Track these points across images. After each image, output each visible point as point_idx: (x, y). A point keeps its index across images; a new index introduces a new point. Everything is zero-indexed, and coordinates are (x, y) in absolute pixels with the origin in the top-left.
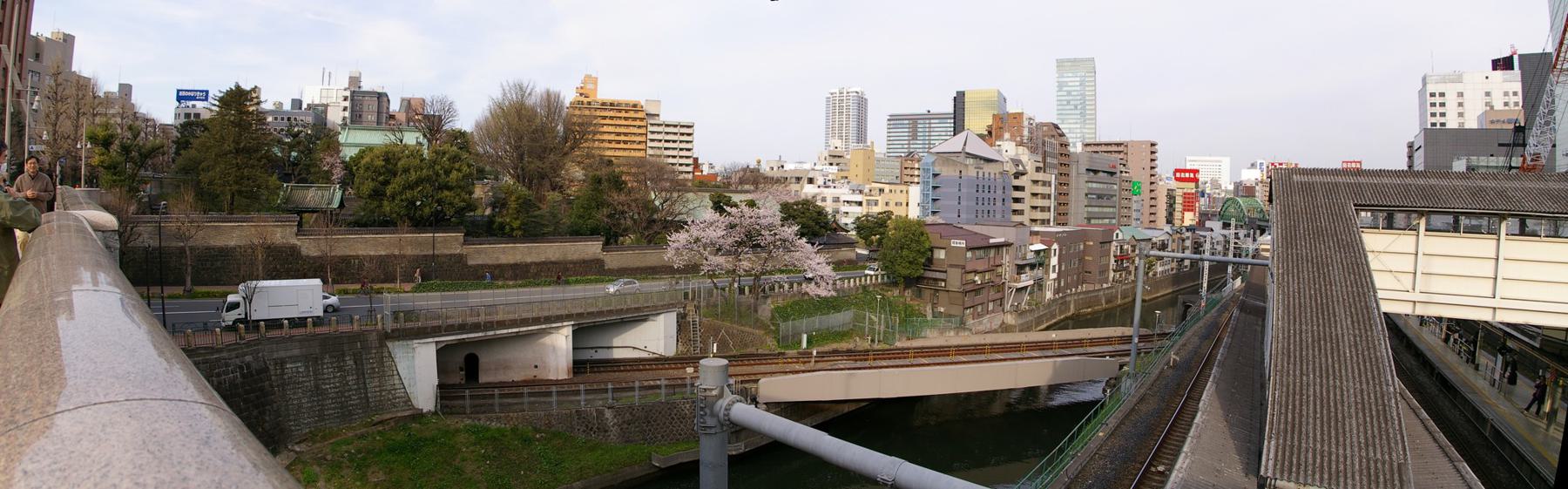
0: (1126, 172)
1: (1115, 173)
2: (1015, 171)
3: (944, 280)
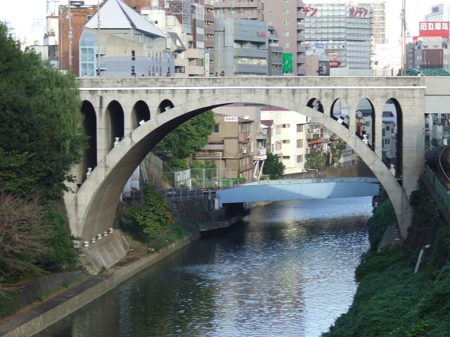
0: (275, 41)
1: (263, 43)
2: (176, 48)
3: (222, 151)
